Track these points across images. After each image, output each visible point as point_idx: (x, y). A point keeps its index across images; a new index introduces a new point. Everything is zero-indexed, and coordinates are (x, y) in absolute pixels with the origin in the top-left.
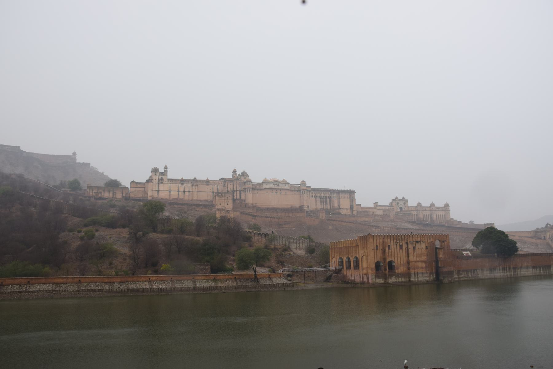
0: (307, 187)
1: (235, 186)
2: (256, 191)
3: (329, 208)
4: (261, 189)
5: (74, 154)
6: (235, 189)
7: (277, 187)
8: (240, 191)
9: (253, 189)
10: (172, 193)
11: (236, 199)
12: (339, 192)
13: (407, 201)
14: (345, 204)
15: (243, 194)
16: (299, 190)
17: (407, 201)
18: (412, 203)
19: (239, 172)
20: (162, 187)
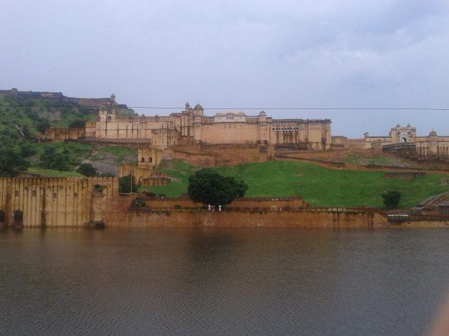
0: (267, 118)
1: (183, 122)
2: (206, 126)
3: (294, 142)
4: (211, 124)
5: (113, 96)
6: (183, 125)
7: (231, 121)
8: (189, 128)
9: (202, 124)
10: (120, 132)
11: (185, 136)
12: (308, 122)
13: (414, 130)
14: (315, 136)
15: (191, 131)
16: (257, 123)
17: (414, 130)
18: (422, 132)
19: (193, 106)
20: (110, 126)
